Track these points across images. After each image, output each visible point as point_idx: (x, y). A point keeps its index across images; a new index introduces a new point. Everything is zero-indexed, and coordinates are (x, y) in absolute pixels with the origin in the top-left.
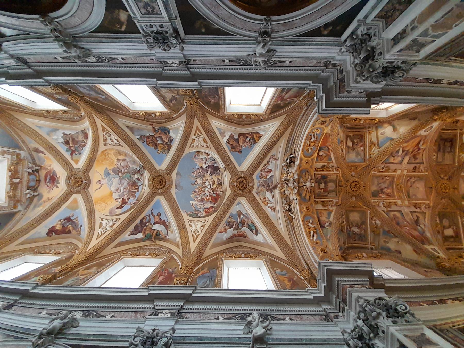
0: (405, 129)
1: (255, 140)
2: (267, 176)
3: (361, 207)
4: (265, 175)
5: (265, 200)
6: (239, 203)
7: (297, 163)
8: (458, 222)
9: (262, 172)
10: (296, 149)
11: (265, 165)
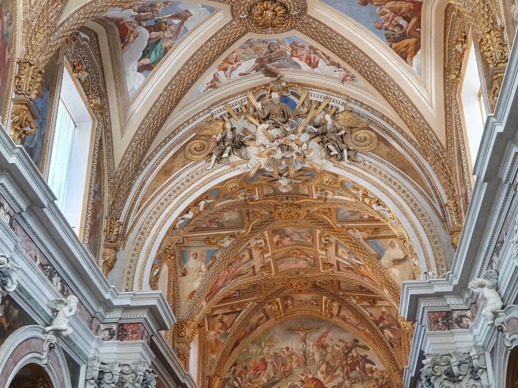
0: (394, 276)
1: (397, 40)
2: (297, 57)
4: (300, 53)
5: (233, 61)
6: (212, 11)
7: (330, 167)
8: (248, 297)
9: (308, 49)
10: (362, 163)
11: (328, 58)
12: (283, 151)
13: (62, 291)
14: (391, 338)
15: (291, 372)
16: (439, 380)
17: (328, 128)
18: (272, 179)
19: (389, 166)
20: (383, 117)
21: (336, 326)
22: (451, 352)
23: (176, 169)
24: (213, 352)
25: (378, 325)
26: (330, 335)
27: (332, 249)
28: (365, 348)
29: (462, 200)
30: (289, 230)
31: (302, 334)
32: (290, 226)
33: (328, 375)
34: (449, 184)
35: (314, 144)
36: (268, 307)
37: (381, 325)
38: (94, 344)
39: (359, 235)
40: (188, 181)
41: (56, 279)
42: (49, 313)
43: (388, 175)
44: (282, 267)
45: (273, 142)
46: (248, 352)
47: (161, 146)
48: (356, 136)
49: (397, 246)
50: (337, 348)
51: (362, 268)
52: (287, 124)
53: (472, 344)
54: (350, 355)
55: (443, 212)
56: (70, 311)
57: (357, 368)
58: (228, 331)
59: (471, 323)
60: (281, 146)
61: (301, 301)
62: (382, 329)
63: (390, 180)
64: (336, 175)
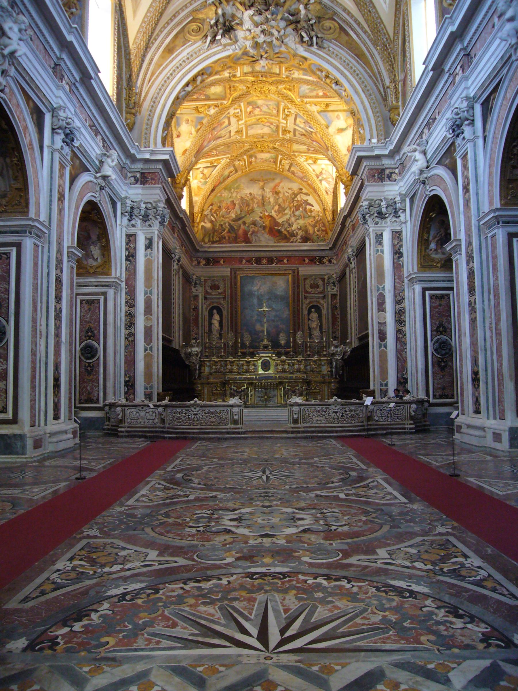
3: (231, 95)
7: (301, 51)
8: (223, 155)
12: (265, 35)
13: (104, 146)
14: (326, 188)
15: (252, 211)
16: (372, 217)
17: (302, 17)
18: (254, 59)
19: (347, 53)
20: (345, 10)
21: (287, 178)
22: (382, 198)
23: (177, 48)
25: (318, 178)
26: (282, 184)
27: (291, 119)
28: (306, 194)
29: (401, 84)
30: (260, 102)
31: (261, 184)
32: (262, 99)
33: (279, 213)
34: (392, 70)
35: (290, 30)
36: (237, 163)
37: (320, 178)
38: (124, 187)
39: (314, 109)
40: (188, 59)
41: (99, 137)
42: (97, 163)
43: (346, 61)
44: (251, 132)
45: (257, 27)
46: (221, 196)
47: (164, 27)
48: (322, 25)
49: (342, 118)
50: (287, 194)
51: (313, 134)
52: (268, 12)
53: (398, 193)
54: (296, 199)
55: (385, 92)
56: (113, 161)
57: (301, 209)
59: (397, 178)
60: (263, 31)
61: (262, 159)
62: (321, 181)
63: (348, 65)
64: (306, 59)
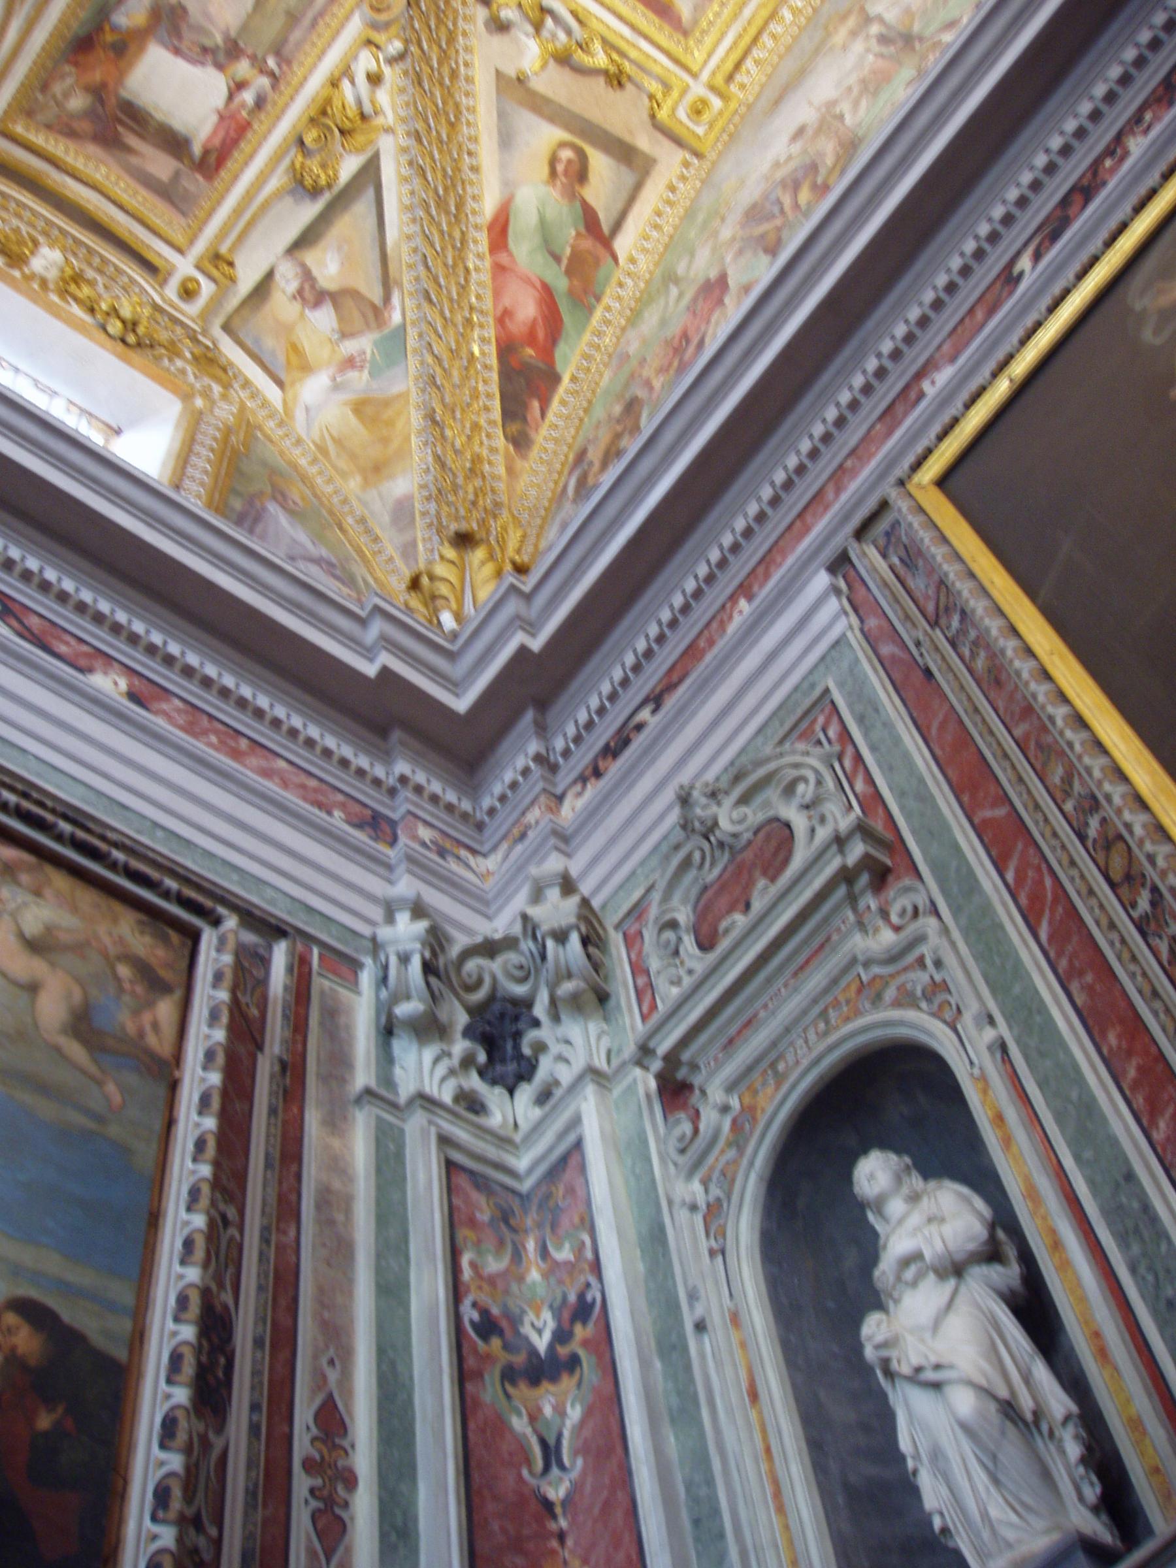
24: (376, 471)
58: (396, 318)
